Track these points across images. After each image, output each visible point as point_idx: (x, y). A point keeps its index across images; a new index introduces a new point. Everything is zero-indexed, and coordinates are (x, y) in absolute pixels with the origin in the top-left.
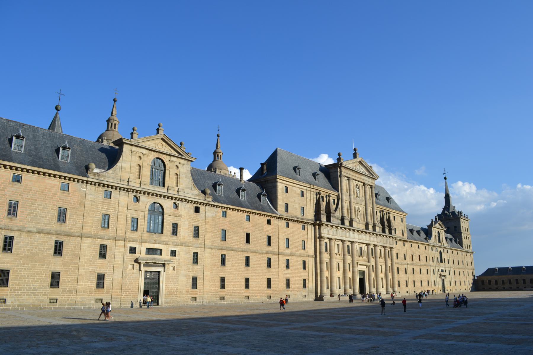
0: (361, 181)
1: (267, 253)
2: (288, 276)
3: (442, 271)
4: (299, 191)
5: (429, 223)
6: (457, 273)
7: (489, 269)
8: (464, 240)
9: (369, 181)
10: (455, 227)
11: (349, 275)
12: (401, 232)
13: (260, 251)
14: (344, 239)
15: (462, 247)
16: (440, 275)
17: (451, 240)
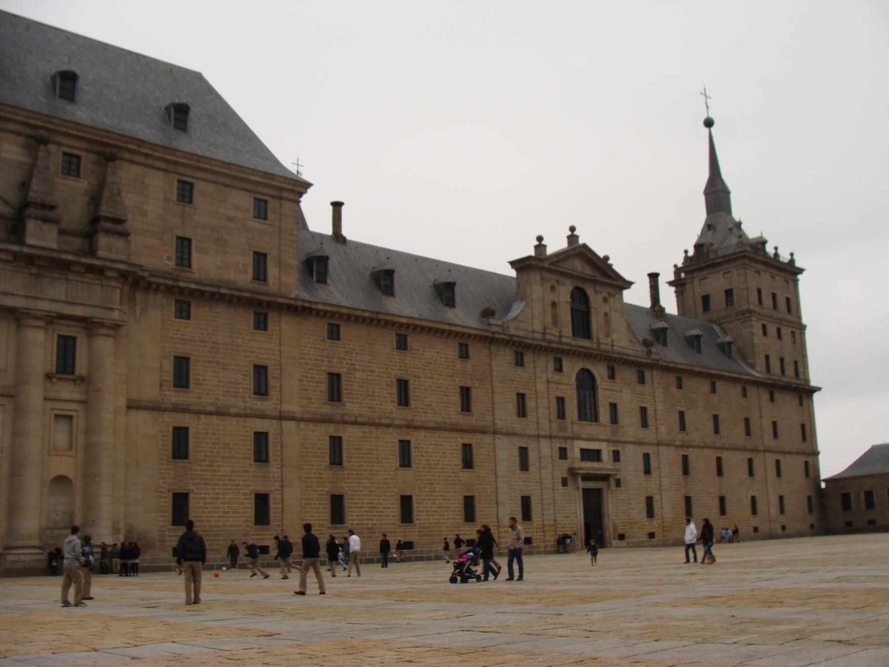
3: (592, 455)
10: (729, 293)
12: (248, 261)
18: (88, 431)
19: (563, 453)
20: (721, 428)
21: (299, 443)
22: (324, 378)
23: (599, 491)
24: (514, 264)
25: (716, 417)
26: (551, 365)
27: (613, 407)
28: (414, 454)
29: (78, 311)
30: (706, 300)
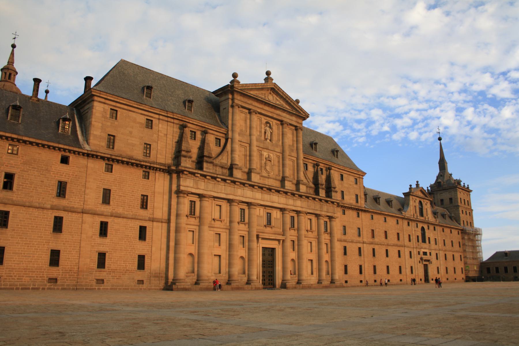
0: (275, 116)
1: (53, 208)
2: (102, 249)
3: (425, 253)
4: (142, 119)
5: (407, 190)
6: (450, 257)
7: (497, 253)
8: (461, 215)
9: (293, 120)
10: (451, 199)
11: (241, 251)
12: (354, 197)
13: (37, 205)
14: (231, 197)
15: (460, 224)
16: (421, 259)
17: (443, 216)
18: (331, 248)
19: (419, 254)
20: (454, 245)
21: (367, 249)
22: (370, 231)
23: (427, 265)
24: (404, 194)
25: (452, 241)
26: (416, 225)
27: (429, 238)
28: (389, 253)
29: (329, 214)
30: (442, 200)
